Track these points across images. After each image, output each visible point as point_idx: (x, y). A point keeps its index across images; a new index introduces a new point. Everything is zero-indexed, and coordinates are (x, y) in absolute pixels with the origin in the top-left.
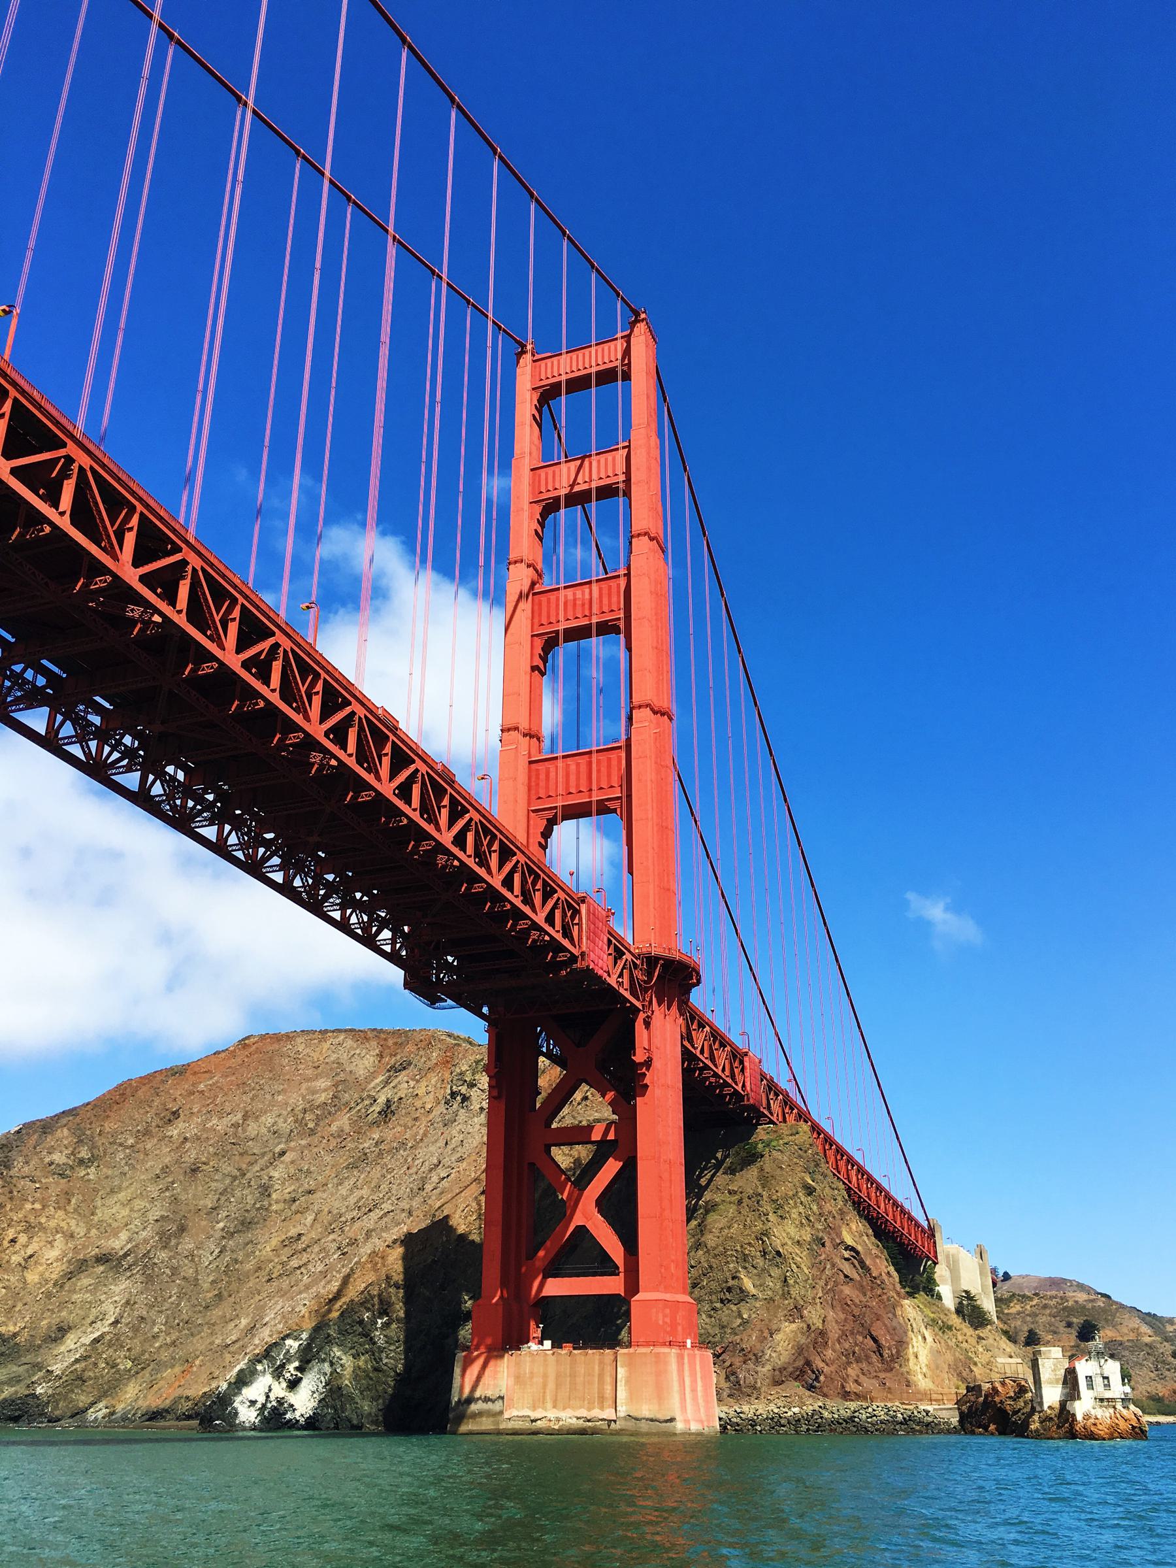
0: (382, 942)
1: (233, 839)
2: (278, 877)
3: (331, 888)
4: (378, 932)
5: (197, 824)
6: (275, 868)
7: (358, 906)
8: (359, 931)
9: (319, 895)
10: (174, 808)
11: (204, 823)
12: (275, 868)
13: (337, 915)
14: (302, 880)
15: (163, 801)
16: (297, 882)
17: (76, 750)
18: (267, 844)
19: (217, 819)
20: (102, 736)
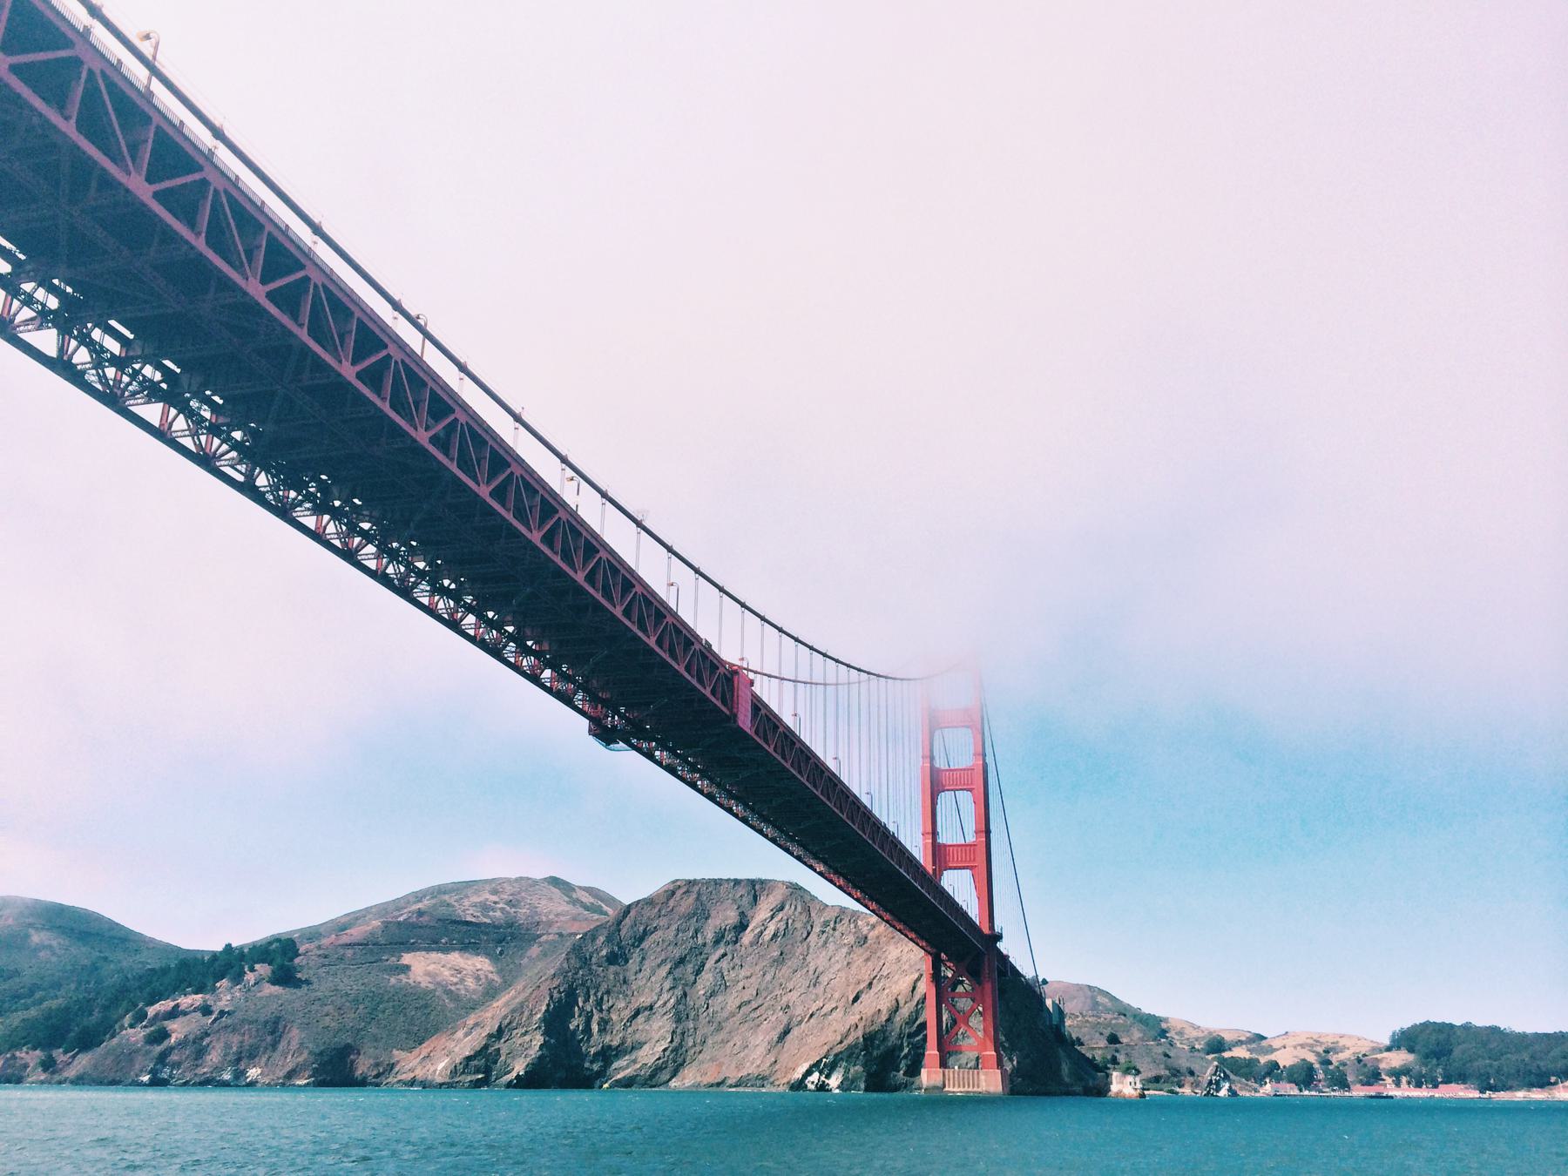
0: (467, 626)
1: (331, 528)
2: (372, 565)
3: (421, 574)
4: (462, 620)
5: (299, 514)
6: (370, 556)
7: (444, 592)
8: (446, 616)
9: (409, 582)
10: (277, 498)
11: (306, 513)
12: (370, 556)
13: (425, 601)
14: (336, 526)
15: (268, 492)
16: (390, 570)
17: (188, 442)
18: (364, 534)
19: (318, 510)
20: (214, 430)
